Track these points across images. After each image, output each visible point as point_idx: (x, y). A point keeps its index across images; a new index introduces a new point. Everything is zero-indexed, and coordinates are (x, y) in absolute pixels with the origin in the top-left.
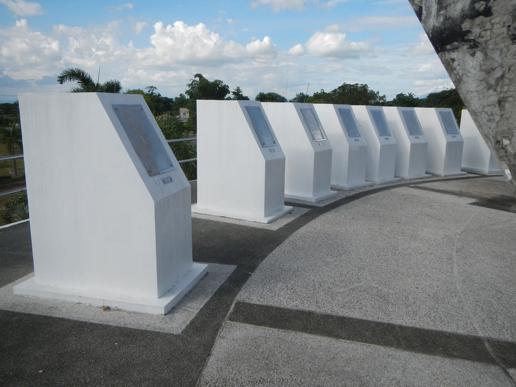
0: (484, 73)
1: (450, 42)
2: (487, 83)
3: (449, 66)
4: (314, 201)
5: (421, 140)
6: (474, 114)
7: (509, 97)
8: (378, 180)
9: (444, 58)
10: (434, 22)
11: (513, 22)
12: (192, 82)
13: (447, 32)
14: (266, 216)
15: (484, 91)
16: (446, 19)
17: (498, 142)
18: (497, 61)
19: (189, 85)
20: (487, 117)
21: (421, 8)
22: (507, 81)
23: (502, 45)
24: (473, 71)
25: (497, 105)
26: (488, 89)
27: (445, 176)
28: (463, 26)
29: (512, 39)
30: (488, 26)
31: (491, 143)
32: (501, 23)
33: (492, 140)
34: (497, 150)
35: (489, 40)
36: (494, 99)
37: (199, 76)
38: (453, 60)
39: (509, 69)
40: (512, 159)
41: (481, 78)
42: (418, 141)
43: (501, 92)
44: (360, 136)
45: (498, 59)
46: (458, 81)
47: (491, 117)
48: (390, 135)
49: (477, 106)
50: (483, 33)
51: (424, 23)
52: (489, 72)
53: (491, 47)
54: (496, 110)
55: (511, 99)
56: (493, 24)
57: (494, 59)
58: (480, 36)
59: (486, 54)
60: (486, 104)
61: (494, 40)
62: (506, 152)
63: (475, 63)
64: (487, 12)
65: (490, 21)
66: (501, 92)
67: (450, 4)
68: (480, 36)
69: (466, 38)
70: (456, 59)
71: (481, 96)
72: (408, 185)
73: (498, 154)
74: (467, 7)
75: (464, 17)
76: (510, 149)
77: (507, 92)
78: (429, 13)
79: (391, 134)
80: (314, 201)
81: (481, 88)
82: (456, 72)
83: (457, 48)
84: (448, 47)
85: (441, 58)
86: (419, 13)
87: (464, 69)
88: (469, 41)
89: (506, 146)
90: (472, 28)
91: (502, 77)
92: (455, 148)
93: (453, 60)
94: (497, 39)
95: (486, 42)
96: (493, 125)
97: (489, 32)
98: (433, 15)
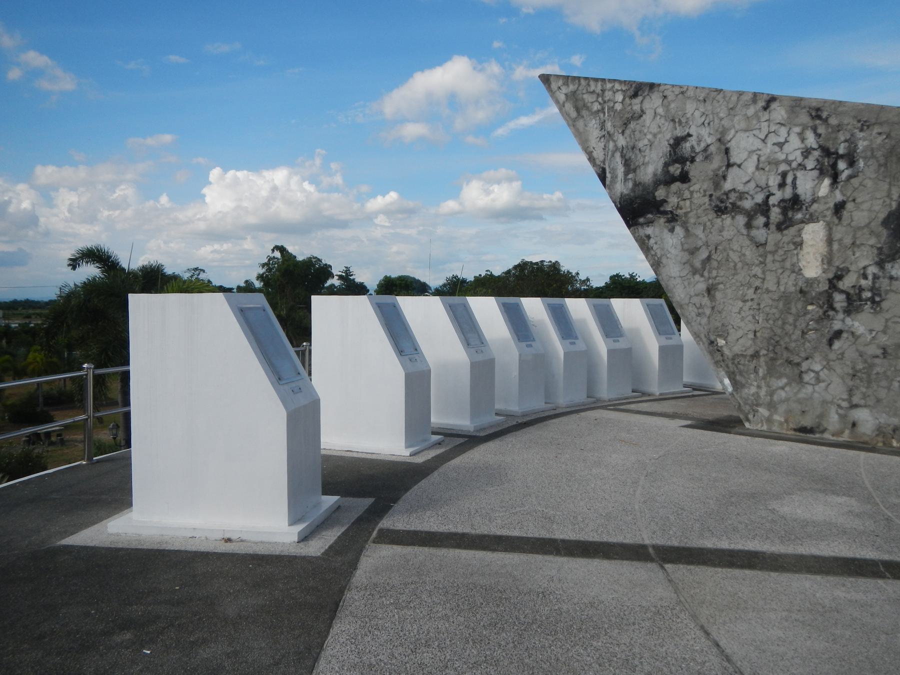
0: (687, 253)
1: (642, 215)
2: (692, 266)
3: (644, 244)
4: (472, 430)
5: (622, 344)
7: (719, 284)
8: (563, 400)
9: (637, 235)
10: (621, 188)
11: (715, 190)
12: (269, 260)
13: (638, 201)
14: (407, 447)
15: (689, 276)
16: (636, 184)
17: (712, 342)
18: (701, 239)
19: (263, 265)
20: (696, 310)
21: (604, 170)
22: (715, 264)
23: (705, 219)
24: (673, 251)
25: (706, 295)
26: (694, 274)
27: (661, 394)
28: (657, 194)
29: (716, 212)
30: (687, 194)
31: (704, 344)
32: (702, 191)
33: (704, 339)
34: (711, 353)
35: (689, 212)
36: (702, 286)
37: (282, 249)
38: (649, 237)
39: (716, 248)
40: (730, 365)
41: (684, 260)
43: (709, 278)
44: (534, 340)
45: (701, 235)
46: (656, 265)
47: (700, 311)
49: (683, 296)
50: (682, 203)
51: (609, 189)
52: (693, 252)
53: (692, 221)
54: (706, 301)
55: (721, 286)
56: (692, 193)
57: (697, 236)
58: (678, 207)
60: (692, 293)
61: (695, 212)
62: (722, 355)
63: (675, 241)
64: (684, 178)
65: (688, 189)
66: (709, 278)
67: (639, 166)
68: (678, 207)
69: (662, 209)
70: (652, 236)
71: (686, 283)
72: (605, 407)
73: (713, 358)
74: (660, 170)
75: (657, 183)
76: (726, 351)
77: (716, 277)
78: (614, 177)
79: (579, 337)
80: (472, 430)
81: (684, 273)
82: (653, 253)
83: (652, 222)
84: (641, 220)
85: (633, 234)
86: (602, 177)
87: (663, 249)
89: (722, 347)
90: (667, 196)
91: (709, 258)
92: (671, 355)
93: (649, 237)
94: (699, 211)
95: (686, 214)
96: (704, 321)
97: (688, 202)
98: (619, 179)
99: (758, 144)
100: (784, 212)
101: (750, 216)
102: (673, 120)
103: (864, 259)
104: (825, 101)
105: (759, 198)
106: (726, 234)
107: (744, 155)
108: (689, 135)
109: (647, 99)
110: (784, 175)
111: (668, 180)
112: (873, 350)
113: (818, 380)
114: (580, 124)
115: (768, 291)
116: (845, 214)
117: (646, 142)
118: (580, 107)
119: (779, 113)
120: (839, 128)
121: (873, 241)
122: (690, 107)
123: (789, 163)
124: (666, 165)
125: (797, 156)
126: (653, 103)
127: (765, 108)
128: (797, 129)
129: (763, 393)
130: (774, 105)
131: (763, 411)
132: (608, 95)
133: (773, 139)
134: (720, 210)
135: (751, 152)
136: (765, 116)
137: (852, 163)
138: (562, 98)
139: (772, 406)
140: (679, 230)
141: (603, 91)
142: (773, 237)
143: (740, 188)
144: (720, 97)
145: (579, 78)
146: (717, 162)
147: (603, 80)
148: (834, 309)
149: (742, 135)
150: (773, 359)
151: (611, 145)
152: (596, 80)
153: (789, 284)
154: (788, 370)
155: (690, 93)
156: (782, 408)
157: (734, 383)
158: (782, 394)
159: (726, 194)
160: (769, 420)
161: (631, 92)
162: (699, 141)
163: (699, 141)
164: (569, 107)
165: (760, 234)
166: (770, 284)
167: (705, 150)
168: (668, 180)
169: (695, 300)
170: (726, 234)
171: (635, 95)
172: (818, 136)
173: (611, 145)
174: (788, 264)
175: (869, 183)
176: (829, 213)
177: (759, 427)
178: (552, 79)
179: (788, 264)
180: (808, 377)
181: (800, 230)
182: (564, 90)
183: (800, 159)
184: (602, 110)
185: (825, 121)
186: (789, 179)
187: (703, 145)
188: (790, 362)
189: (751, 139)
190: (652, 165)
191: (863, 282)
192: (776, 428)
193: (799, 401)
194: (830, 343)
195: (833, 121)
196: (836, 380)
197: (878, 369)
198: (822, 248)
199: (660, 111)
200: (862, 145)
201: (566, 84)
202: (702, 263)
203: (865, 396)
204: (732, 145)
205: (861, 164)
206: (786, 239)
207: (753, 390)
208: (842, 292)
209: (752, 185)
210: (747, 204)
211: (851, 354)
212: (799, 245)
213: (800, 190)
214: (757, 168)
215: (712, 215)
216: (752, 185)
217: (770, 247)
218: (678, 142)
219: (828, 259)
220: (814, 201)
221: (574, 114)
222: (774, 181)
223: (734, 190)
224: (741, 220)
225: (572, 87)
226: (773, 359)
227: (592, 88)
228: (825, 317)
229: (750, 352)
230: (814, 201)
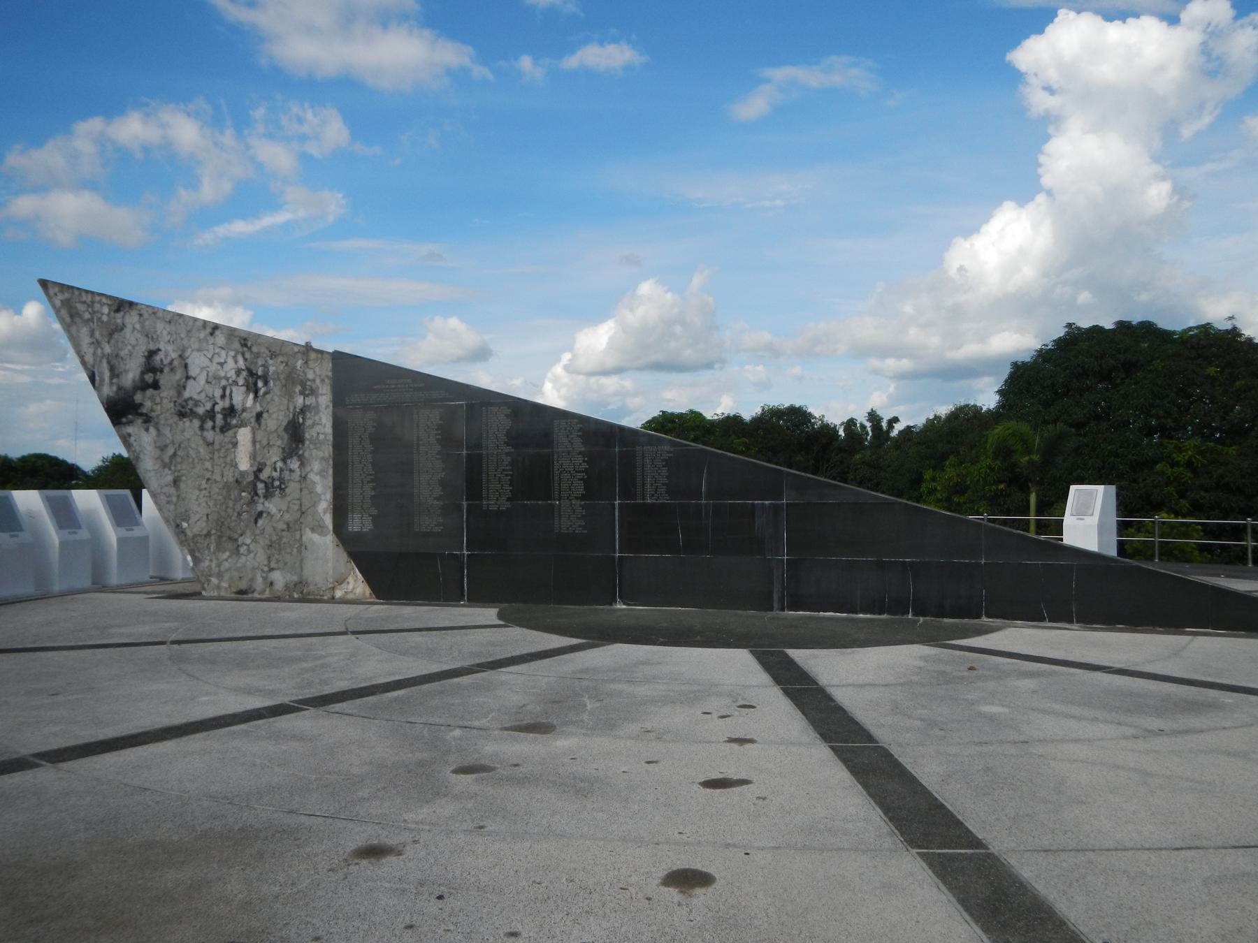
3: (125, 439)
5: (137, 532)
6: (154, 495)
10: (108, 390)
16: (120, 388)
22: (179, 459)
23: (171, 421)
30: (158, 400)
34: (177, 534)
36: (170, 478)
38: (130, 435)
42: (130, 534)
44: (21, 530)
45: (169, 435)
48: (79, 527)
52: (163, 448)
54: (173, 490)
59: (158, 430)
64: (156, 386)
68: (152, 410)
76: (189, 533)
78: (102, 380)
84: (124, 420)
86: (92, 379)
88: (141, 414)
91: (175, 454)
93: (130, 435)
96: (172, 507)
99: (207, 363)
100: (225, 419)
101: (203, 421)
102: (147, 336)
103: (274, 456)
104: (250, 333)
105: (208, 406)
106: (187, 434)
107: (197, 371)
108: (159, 350)
109: (127, 316)
110: (224, 389)
111: (143, 386)
112: (282, 526)
113: (249, 551)
114: (74, 329)
115: (216, 482)
116: (263, 421)
117: (126, 352)
118: (74, 314)
119: (220, 339)
120: (258, 355)
121: (279, 443)
122: (160, 326)
123: (227, 379)
124: (143, 373)
125: (232, 374)
126: (132, 319)
127: (212, 334)
128: (232, 353)
129: (213, 566)
130: (217, 332)
131: (214, 580)
132: (97, 306)
133: (217, 359)
134: (182, 415)
135: (203, 368)
136: (211, 340)
137: (266, 383)
138: (58, 303)
139: (220, 575)
140: (152, 430)
141: (93, 302)
142: (219, 438)
143: (195, 397)
144: (181, 321)
145: (72, 287)
146: (179, 375)
147: (92, 293)
148: (257, 494)
149: (195, 353)
150: (220, 537)
151: (99, 351)
152: (87, 292)
153: (230, 476)
154: (230, 545)
155: (160, 314)
156: (226, 576)
157: (195, 559)
158: (226, 565)
159: (186, 401)
160: (218, 587)
161: (115, 307)
162: (166, 356)
163: (166, 356)
164: (64, 312)
165: (210, 435)
167: (171, 363)
168: (143, 386)
169: (165, 490)
170: (187, 434)
171: (118, 310)
172: (246, 360)
173: (99, 351)
174: (228, 460)
175: (276, 399)
176: (253, 420)
177: (212, 594)
178: (50, 285)
179: (228, 460)
180: (243, 550)
181: (235, 433)
182: (60, 297)
183: (234, 377)
184: (92, 320)
185: (250, 349)
186: (228, 393)
187: (169, 359)
188: (230, 538)
189: (203, 358)
190: (132, 372)
191: (276, 474)
192: (223, 594)
193: (238, 569)
194: (256, 522)
195: (255, 349)
196: (261, 551)
197: (285, 540)
198: (249, 446)
199: (138, 326)
200: (272, 369)
201: (62, 291)
202: (171, 459)
203: (278, 561)
204: (189, 361)
205: (271, 383)
206: (226, 440)
207: (207, 563)
208: (262, 481)
209: (203, 395)
210: (201, 410)
211: (269, 530)
212: (235, 444)
213: (235, 402)
214: (208, 382)
215: (176, 418)
216: (203, 395)
217: (216, 446)
218: (151, 354)
219: (253, 456)
220: (244, 410)
221: (68, 319)
222: (218, 393)
223: (191, 398)
224: (197, 423)
225: (67, 295)
226: (220, 537)
227: (84, 298)
228: (252, 502)
229: (205, 532)
230: (244, 410)
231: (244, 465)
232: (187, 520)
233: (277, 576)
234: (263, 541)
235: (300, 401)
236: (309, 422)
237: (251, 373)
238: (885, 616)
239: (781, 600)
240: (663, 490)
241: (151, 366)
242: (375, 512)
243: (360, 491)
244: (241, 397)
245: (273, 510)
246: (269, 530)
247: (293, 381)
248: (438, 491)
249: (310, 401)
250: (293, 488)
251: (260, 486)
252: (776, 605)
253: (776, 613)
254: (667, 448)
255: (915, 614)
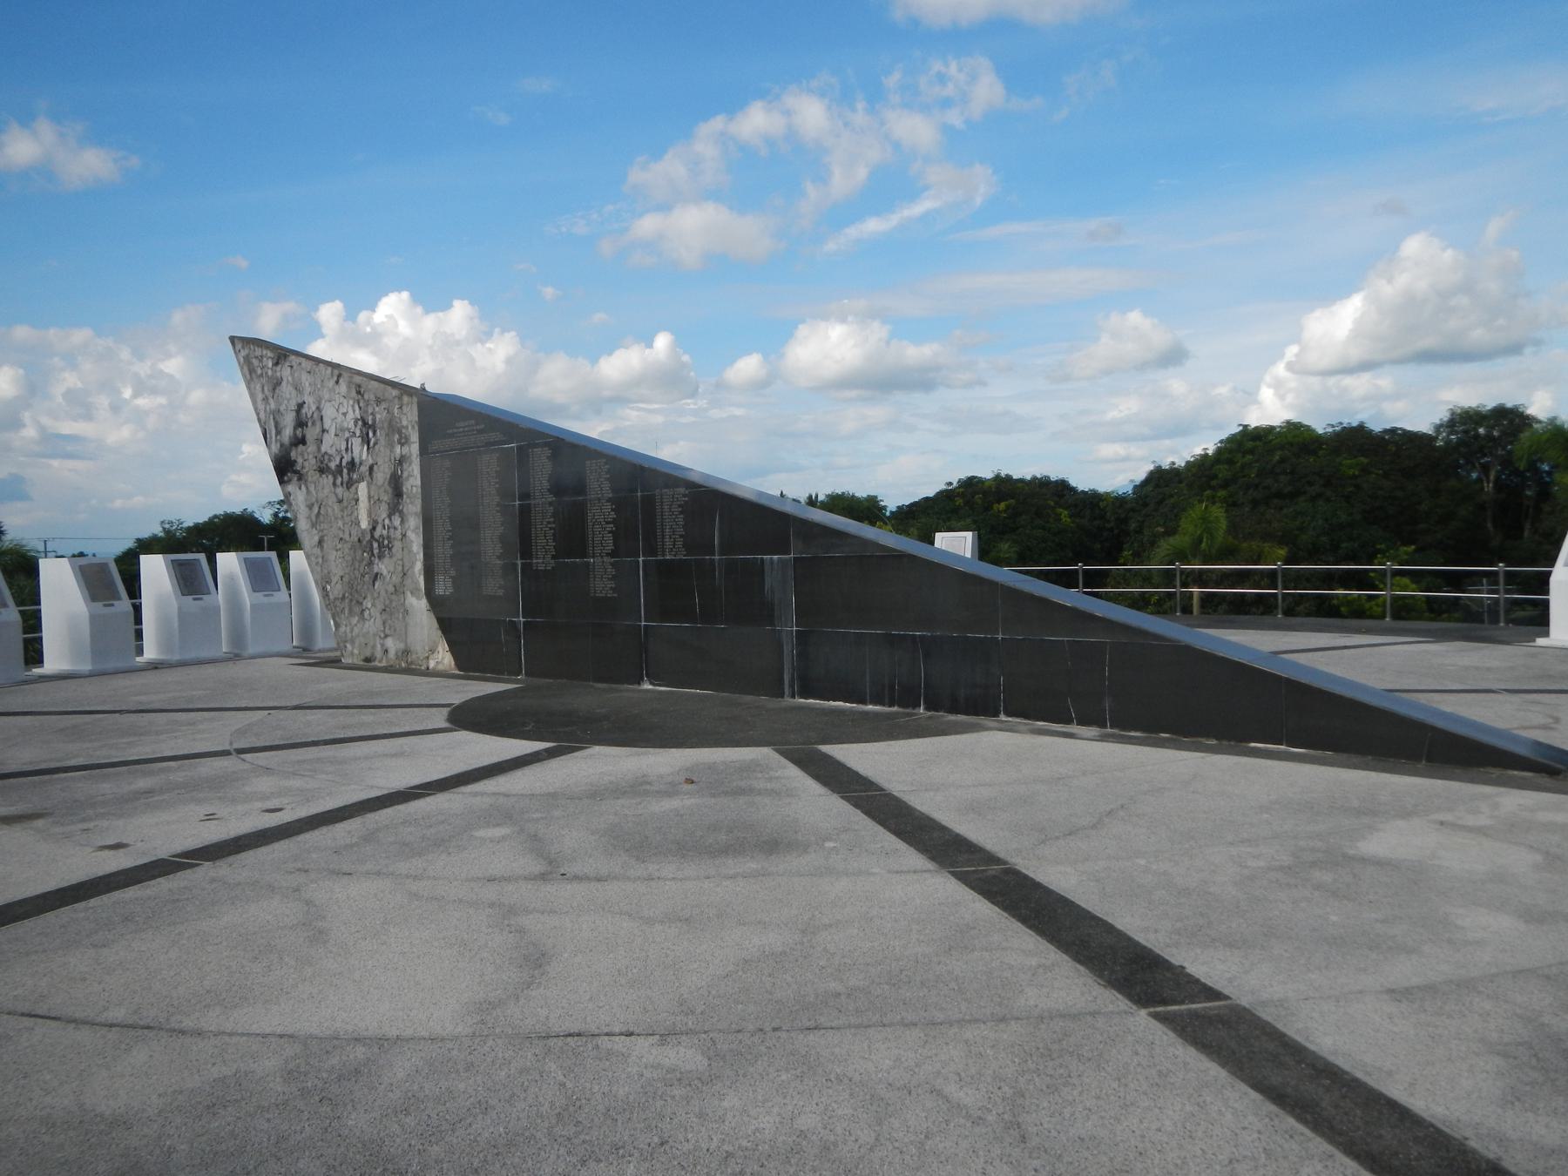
36: (316, 538)
52: (310, 507)
54: (317, 551)
64: (303, 441)
88: (296, 472)
99: (335, 414)
106: (326, 491)
118: (252, 371)
119: (343, 388)
120: (367, 403)
125: (351, 425)
126: (285, 372)
139: (352, 642)
146: (318, 429)
154: (357, 609)
157: (337, 625)
158: (356, 630)
165: (340, 490)
166: (346, 537)
171: (276, 364)
180: (366, 614)
210: (333, 465)
211: (383, 593)
218: (300, 406)
219: (370, 515)
228: (370, 563)
231: (364, 524)
232: (329, 582)
233: (390, 643)
234: (380, 607)
235: (398, 449)
236: (405, 474)
237: (365, 423)
238: (895, 709)
239: (792, 686)
240: (679, 544)
241: (301, 423)
242: (453, 573)
243: (443, 551)
244: (359, 451)
245: (385, 572)
246: (383, 593)
247: (394, 429)
248: (499, 550)
249: (405, 450)
250: (397, 545)
251: (375, 545)
252: (787, 690)
253: (788, 701)
254: (682, 490)
255: (927, 709)
